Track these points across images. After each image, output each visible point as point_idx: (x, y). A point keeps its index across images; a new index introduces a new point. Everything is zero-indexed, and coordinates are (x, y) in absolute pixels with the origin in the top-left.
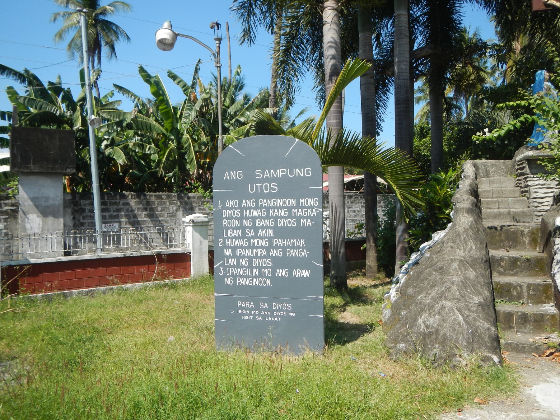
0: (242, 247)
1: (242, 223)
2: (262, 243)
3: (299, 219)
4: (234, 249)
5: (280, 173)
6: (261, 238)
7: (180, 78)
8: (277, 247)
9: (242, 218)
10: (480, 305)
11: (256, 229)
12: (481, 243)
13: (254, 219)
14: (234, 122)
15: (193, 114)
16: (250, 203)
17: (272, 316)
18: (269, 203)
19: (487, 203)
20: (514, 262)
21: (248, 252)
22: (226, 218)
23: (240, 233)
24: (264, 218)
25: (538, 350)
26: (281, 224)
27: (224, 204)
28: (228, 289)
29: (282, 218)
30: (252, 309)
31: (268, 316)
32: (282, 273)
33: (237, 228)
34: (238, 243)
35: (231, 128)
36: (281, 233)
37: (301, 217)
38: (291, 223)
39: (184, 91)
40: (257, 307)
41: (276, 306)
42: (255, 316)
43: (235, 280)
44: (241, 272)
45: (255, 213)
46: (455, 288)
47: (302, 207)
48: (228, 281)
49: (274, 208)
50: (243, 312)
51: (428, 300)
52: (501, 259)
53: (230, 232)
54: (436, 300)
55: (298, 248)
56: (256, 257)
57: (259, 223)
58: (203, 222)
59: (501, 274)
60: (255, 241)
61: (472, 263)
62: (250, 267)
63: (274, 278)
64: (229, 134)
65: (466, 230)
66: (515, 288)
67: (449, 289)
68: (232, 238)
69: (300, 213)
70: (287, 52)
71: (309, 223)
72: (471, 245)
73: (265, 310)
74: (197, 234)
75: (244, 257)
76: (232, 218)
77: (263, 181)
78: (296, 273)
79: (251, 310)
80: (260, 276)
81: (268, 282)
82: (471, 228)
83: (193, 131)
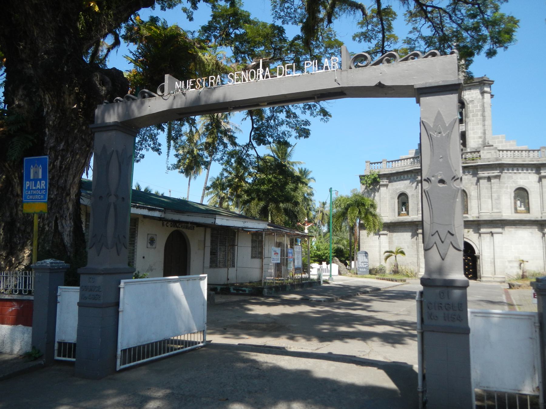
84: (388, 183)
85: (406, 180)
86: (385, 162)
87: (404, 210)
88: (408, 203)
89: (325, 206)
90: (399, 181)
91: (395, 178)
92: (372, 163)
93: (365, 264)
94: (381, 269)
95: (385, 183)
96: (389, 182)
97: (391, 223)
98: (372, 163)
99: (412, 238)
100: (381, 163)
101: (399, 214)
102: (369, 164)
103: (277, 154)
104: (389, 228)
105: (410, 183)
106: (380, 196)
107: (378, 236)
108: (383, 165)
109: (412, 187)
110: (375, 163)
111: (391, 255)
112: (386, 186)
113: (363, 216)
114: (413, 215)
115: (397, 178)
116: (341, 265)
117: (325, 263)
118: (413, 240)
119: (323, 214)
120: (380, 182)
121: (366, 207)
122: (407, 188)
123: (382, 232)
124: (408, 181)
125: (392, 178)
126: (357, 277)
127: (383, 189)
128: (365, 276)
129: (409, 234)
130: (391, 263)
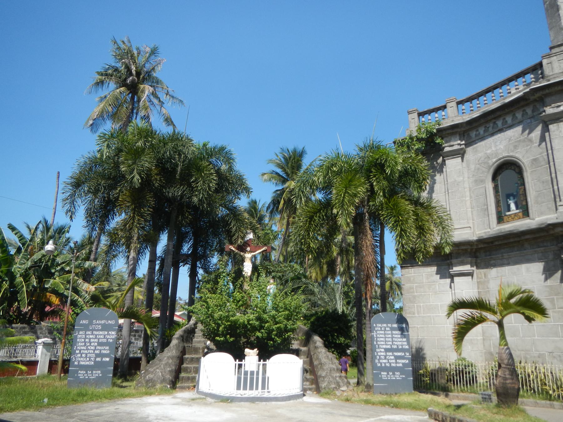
0: (84, 350)
1: (85, 340)
2: (92, 348)
3: (107, 339)
4: (80, 350)
5: (103, 322)
6: (92, 346)
7: (18, 230)
8: (98, 350)
9: (85, 339)
10: (170, 371)
11: (90, 343)
12: (179, 351)
13: (90, 339)
14: (60, 269)
15: (29, 263)
16: (89, 333)
17: (92, 376)
18: (97, 333)
19: (197, 336)
20: (192, 359)
21: (86, 352)
22: (79, 338)
23: (84, 344)
24: (94, 339)
25: (189, 388)
26: (100, 341)
27: (79, 332)
28: (76, 366)
29: (101, 338)
30: (85, 374)
31: (90, 376)
32: (98, 359)
33: (83, 342)
34: (82, 348)
35: (57, 273)
36: (100, 344)
37: (108, 338)
38: (105, 340)
39: (20, 240)
40: (87, 373)
41: (94, 372)
42: (85, 376)
43: (79, 363)
44: (82, 359)
45: (91, 336)
46: (162, 366)
47: (110, 335)
48: (76, 363)
49: (99, 335)
50: (81, 375)
51: (152, 370)
52: (188, 358)
53: (79, 344)
54: (154, 370)
55: (106, 350)
56: (89, 353)
57: (92, 340)
58: (49, 343)
59: (187, 364)
60: (89, 347)
61: (172, 358)
62: (86, 357)
63: (95, 362)
64: (55, 279)
65: (173, 346)
66: (189, 368)
67: (160, 366)
68: (80, 346)
69: (108, 337)
70: (110, 247)
71: (111, 341)
72: (174, 351)
73: (90, 374)
74: (45, 351)
75: (84, 353)
76: (81, 338)
77: (96, 324)
78: (104, 359)
79: (84, 374)
80: (90, 360)
81: (93, 363)
82: (176, 345)
83: (26, 276)
84: (463, 146)
85: (510, 127)
86: (454, 104)
87: (513, 206)
88: (524, 184)
89: (394, 271)
90: (492, 134)
91: (481, 131)
92: (421, 114)
93: (397, 358)
94: (461, 373)
95: (456, 147)
96: (468, 145)
97: (481, 241)
98: (421, 114)
99: (546, 279)
100: (444, 107)
101: (500, 219)
102: (415, 115)
103: (284, 170)
104: (476, 257)
105: (523, 131)
106: (446, 181)
107: (448, 280)
108: (452, 110)
109: (531, 141)
110: (429, 112)
111: (482, 320)
112: (460, 153)
113: (380, 199)
114: (542, 214)
115: (485, 131)
116: (324, 360)
117: (256, 351)
118: (549, 282)
119: (391, 283)
120: (444, 148)
121: (388, 171)
122: (516, 147)
123: (457, 269)
124: (519, 129)
125: (473, 134)
126: (367, 402)
127: (452, 164)
128: (395, 399)
129: (538, 267)
130: (491, 354)
